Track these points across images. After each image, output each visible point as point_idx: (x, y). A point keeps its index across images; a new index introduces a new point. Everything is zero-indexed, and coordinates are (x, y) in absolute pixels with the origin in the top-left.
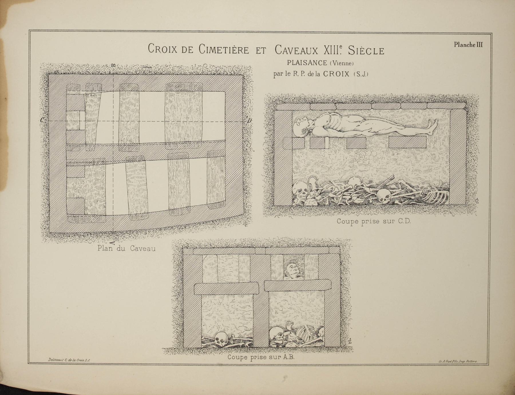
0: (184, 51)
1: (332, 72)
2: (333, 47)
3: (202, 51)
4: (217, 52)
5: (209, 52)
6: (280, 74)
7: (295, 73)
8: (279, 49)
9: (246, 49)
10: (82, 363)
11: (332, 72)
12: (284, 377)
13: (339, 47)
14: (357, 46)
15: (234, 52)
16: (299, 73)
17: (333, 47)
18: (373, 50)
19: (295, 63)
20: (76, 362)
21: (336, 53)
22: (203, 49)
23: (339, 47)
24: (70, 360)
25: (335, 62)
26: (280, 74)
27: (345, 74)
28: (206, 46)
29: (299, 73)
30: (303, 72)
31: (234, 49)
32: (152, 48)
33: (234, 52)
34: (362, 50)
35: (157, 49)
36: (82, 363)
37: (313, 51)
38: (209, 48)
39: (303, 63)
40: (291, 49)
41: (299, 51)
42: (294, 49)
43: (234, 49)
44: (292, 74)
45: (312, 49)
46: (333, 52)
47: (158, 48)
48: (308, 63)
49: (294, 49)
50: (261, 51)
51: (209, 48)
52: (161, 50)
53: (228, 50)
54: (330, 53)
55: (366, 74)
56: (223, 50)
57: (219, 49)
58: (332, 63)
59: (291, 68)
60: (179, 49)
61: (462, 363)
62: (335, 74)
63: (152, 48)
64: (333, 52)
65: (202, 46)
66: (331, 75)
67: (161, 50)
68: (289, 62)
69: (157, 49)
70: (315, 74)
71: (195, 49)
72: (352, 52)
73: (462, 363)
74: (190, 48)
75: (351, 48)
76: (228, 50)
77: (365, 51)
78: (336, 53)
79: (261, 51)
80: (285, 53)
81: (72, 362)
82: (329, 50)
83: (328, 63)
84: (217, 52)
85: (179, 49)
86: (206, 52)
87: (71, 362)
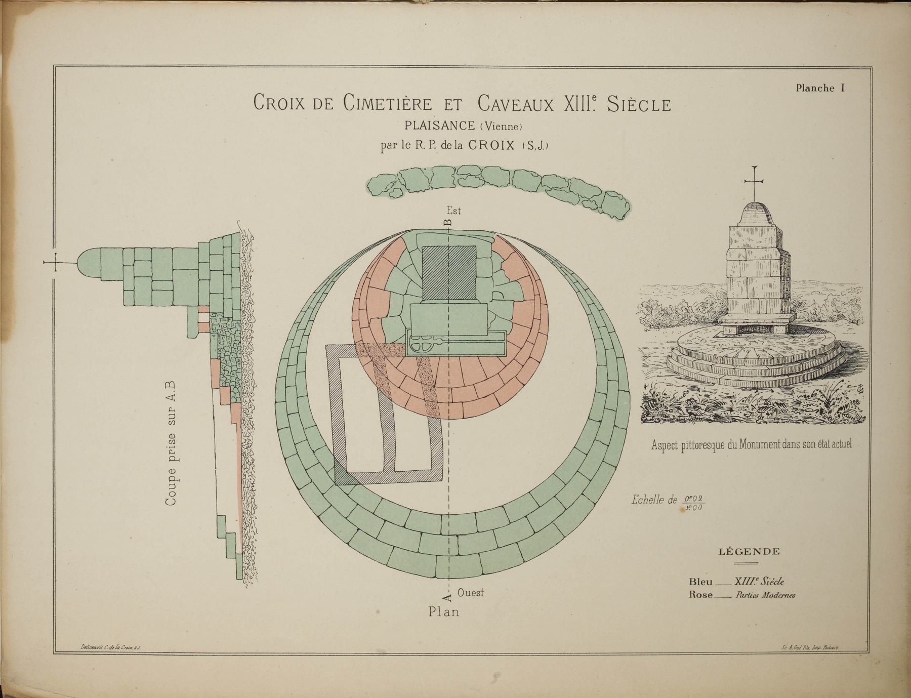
0: (318, 106)
1: (483, 143)
2: (580, 99)
3: (349, 106)
4: (375, 107)
5: (361, 107)
6: (392, 146)
7: (419, 143)
8: (485, 103)
9: (427, 102)
10: (129, 651)
11: (483, 143)
12: (495, 676)
13: (591, 98)
14: (623, 96)
15: (328, 107)
16: (426, 144)
17: (580, 99)
18: (651, 103)
19: (418, 125)
20: (120, 650)
21: (586, 108)
22: (351, 102)
23: (591, 98)
24: (112, 648)
25: (489, 124)
26: (392, 146)
27: (506, 145)
28: (356, 97)
29: (426, 144)
30: (432, 142)
31: (406, 102)
32: (261, 101)
33: (406, 107)
34: (631, 103)
35: (270, 103)
36: (129, 651)
37: (545, 105)
38: (361, 101)
39: (432, 125)
40: (505, 103)
41: (521, 105)
42: (511, 102)
43: (406, 102)
44: (414, 145)
45: (543, 102)
46: (580, 108)
47: (271, 101)
48: (441, 125)
49: (511, 102)
50: (453, 105)
51: (361, 101)
52: (276, 104)
53: (394, 104)
54: (575, 108)
55: (544, 146)
56: (386, 104)
57: (379, 102)
58: (484, 126)
59: (411, 136)
60: (308, 103)
61: (816, 650)
62: (488, 145)
63: (261, 101)
64: (580, 108)
65: (349, 97)
66: (483, 147)
67: (276, 104)
68: (408, 124)
69: (270, 103)
70: (400, 143)
71: (337, 103)
72: (614, 107)
73: (816, 650)
74: (328, 101)
75: (613, 99)
76: (394, 104)
77: (636, 106)
78: (586, 108)
79: (453, 105)
80: (496, 109)
81: (114, 650)
82: (573, 103)
83: (476, 125)
84: (375, 107)
85: (308, 103)
86: (356, 107)
87: (113, 651)
